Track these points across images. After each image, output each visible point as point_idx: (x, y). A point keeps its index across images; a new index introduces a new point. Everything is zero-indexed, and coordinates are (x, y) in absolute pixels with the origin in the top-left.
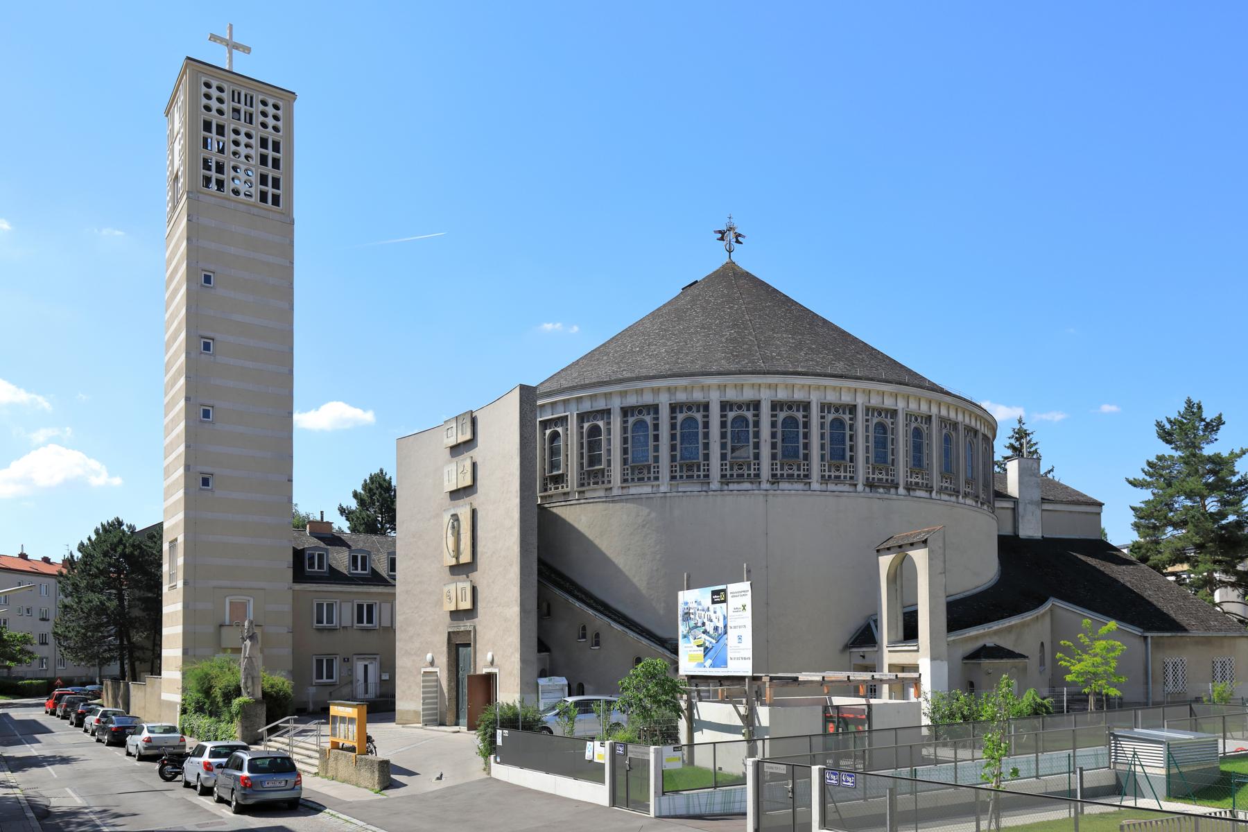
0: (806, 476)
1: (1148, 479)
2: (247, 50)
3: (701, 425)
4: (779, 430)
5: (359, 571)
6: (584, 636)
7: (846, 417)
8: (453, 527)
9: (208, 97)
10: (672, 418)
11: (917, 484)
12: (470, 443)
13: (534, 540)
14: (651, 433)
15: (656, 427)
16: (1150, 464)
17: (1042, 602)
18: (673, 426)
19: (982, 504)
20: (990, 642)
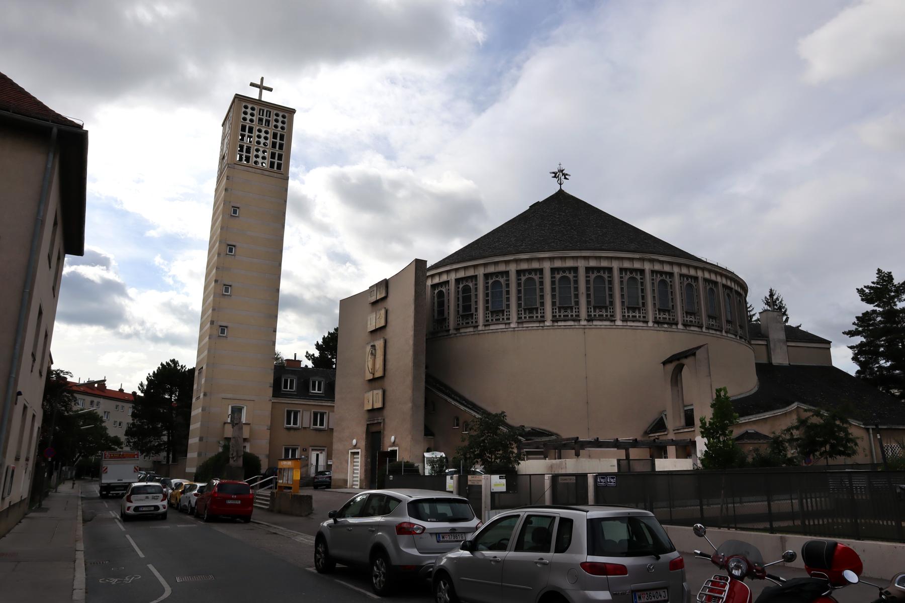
0: (612, 316)
1: (860, 329)
2: (270, 90)
4: (592, 285)
5: (316, 391)
7: (639, 277)
8: (372, 354)
9: (245, 113)
10: (519, 280)
11: (691, 321)
12: (384, 299)
13: (423, 358)
14: (504, 289)
15: (508, 285)
16: (858, 318)
17: (789, 403)
18: (519, 285)
19: (741, 337)
20: (751, 429)
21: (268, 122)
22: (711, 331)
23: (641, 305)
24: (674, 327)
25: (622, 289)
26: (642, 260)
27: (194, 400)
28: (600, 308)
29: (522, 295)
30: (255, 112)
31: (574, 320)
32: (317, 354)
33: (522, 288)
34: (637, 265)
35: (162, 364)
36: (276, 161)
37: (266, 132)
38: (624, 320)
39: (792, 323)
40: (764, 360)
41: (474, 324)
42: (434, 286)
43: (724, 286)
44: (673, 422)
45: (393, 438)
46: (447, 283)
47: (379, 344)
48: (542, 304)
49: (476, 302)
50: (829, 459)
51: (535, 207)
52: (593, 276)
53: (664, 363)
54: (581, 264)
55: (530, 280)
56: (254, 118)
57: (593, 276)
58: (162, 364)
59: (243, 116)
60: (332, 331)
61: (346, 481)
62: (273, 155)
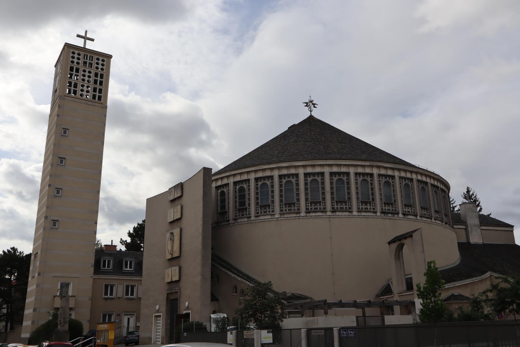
2: (92, 40)
3: (294, 185)
5: (128, 269)
6: (236, 292)
7: (369, 179)
8: (171, 239)
9: (73, 57)
10: (281, 182)
11: (409, 212)
13: (209, 242)
14: (270, 189)
15: (272, 186)
17: (484, 273)
18: (281, 186)
19: (446, 223)
20: (456, 292)
21: (91, 64)
22: (424, 219)
23: (371, 199)
24: (396, 216)
25: (357, 188)
26: (372, 166)
27: (30, 279)
28: (341, 202)
29: (283, 193)
30: (80, 57)
31: (322, 212)
32: (129, 240)
33: (283, 188)
34: (368, 170)
35: (4, 252)
36: (97, 94)
37: (90, 72)
38: (359, 211)
39: (484, 212)
40: (464, 240)
41: (248, 216)
42: (217, 188)
43: (433, 185)
44: (398, 287)
45: (187, 303)
46: (227, 185)
47: (177, 231)
48: (298, 200)
49: (249, 199)
50: (517, 315)
51: (293, 128)
52: (335, 179)
53: (389, 243)
54: (327, 170)
55: (265, 184)
56: (80, 61)
57: (335, 179)
58: (4, 252)
59: (71, 59)
60: (141, 222)
61: (150, 339)
62: (95, 90)
